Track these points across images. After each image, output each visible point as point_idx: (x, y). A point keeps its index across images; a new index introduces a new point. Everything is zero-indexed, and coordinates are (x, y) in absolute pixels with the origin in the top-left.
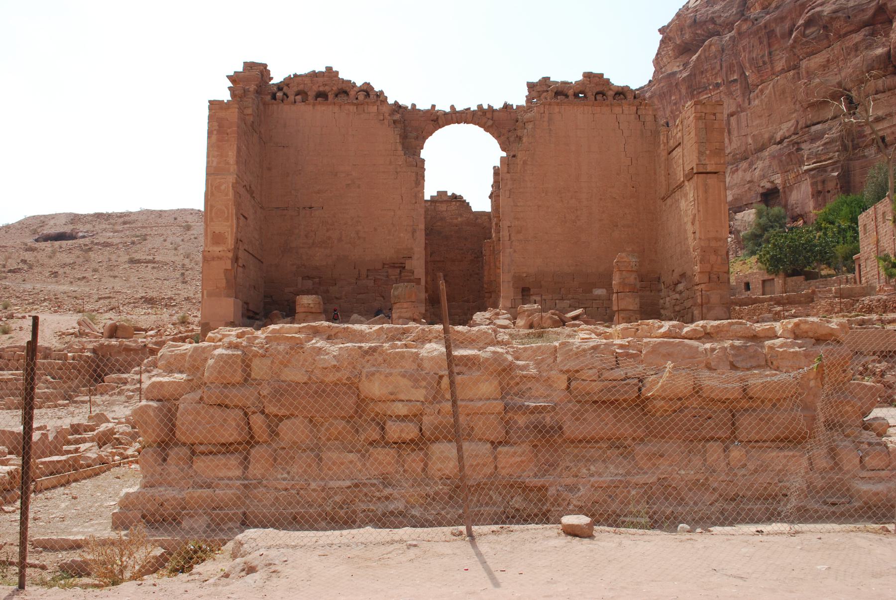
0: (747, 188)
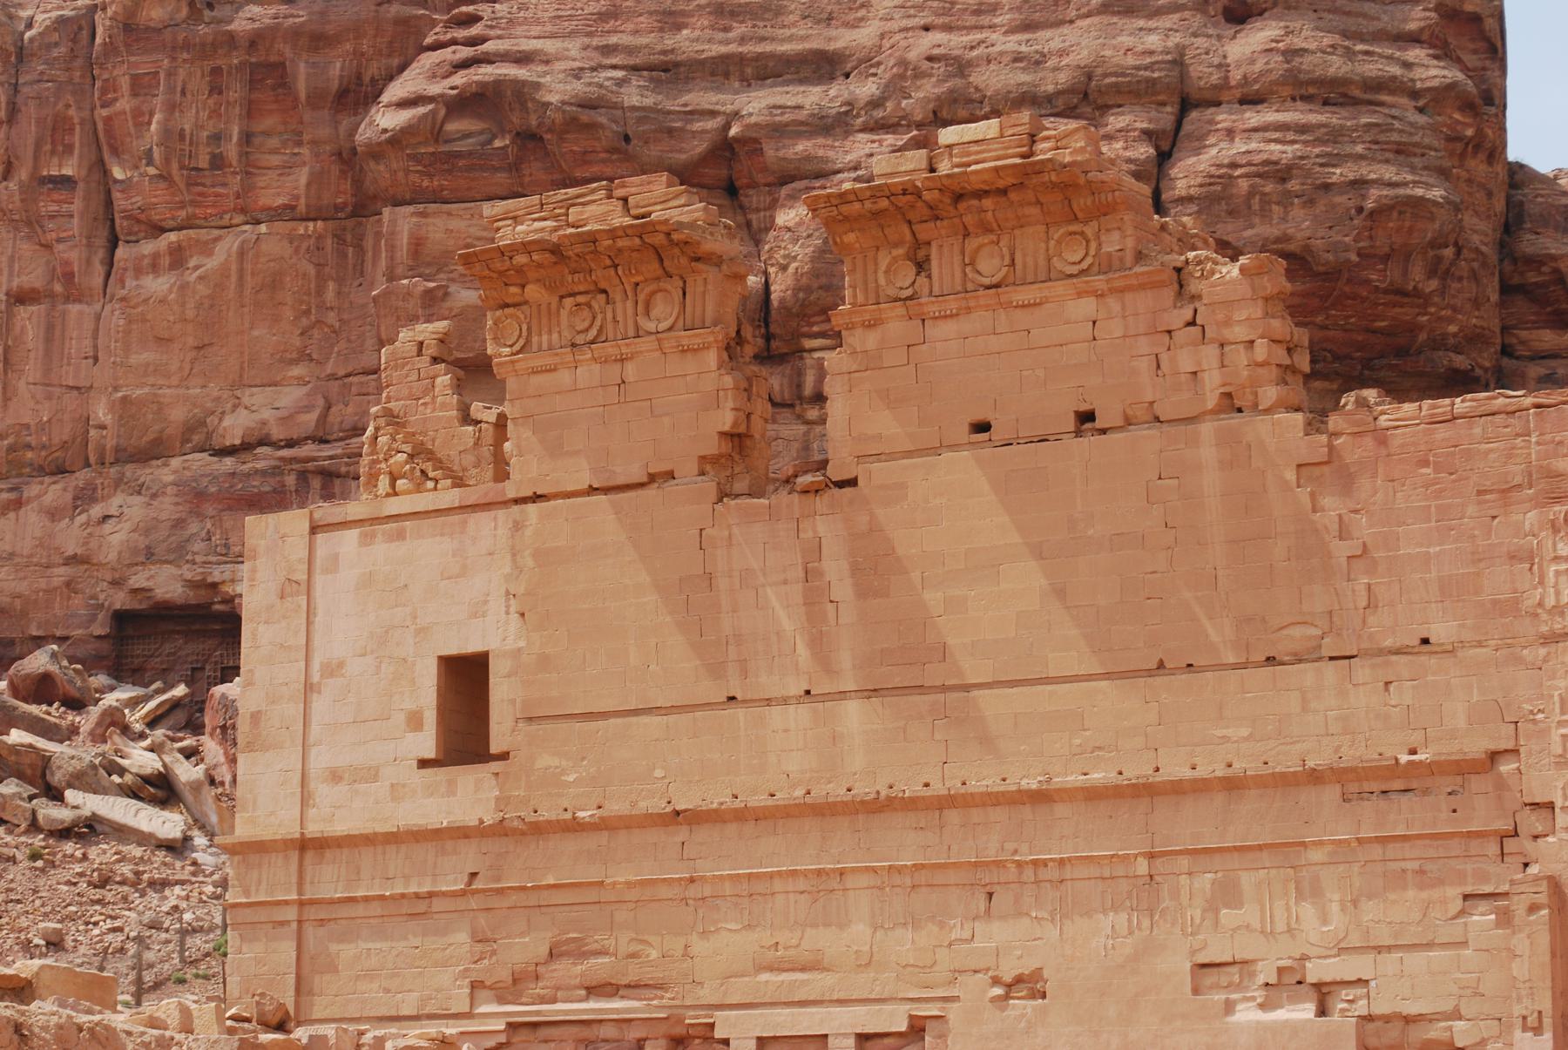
0: (57, 582)
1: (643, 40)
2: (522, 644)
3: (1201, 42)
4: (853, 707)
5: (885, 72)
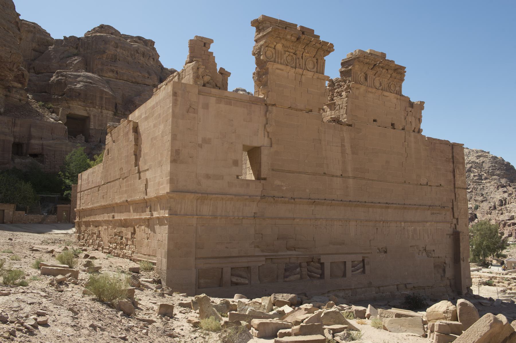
4: (351, 181)
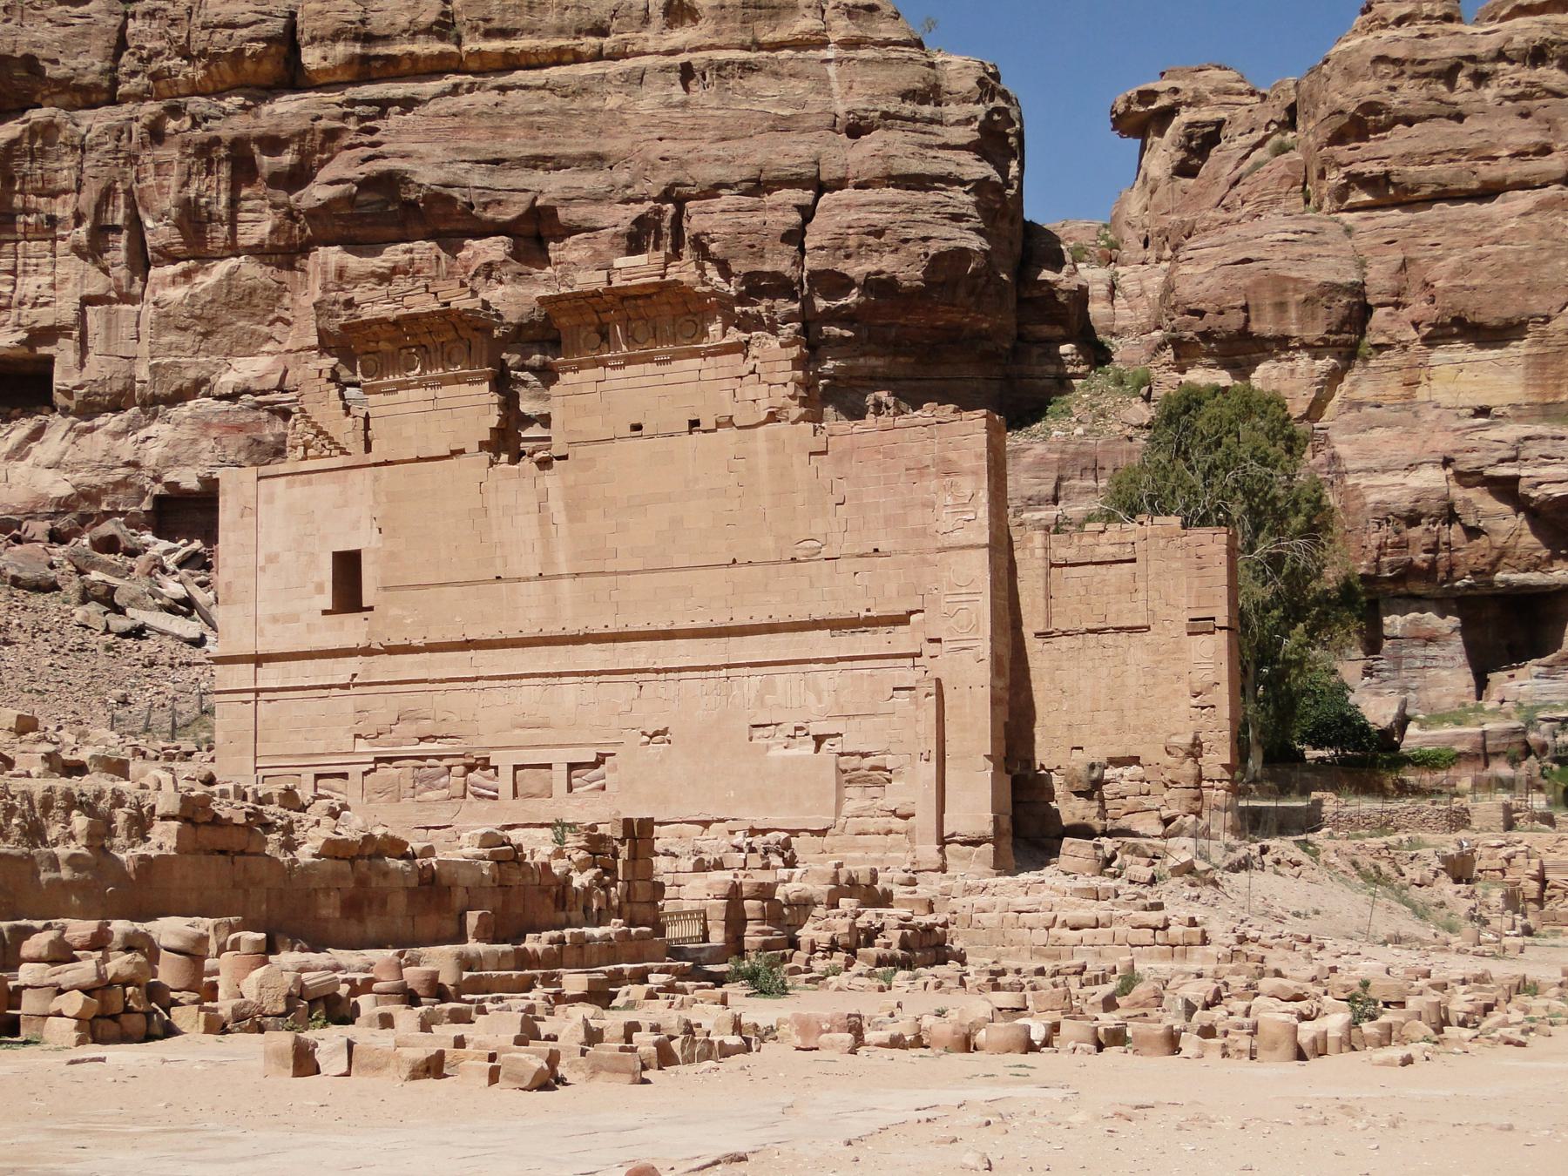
1: (482, 145)
2: (380, 545)
3: (831, 150)
4: (566, 584)
5: (636, 165)
